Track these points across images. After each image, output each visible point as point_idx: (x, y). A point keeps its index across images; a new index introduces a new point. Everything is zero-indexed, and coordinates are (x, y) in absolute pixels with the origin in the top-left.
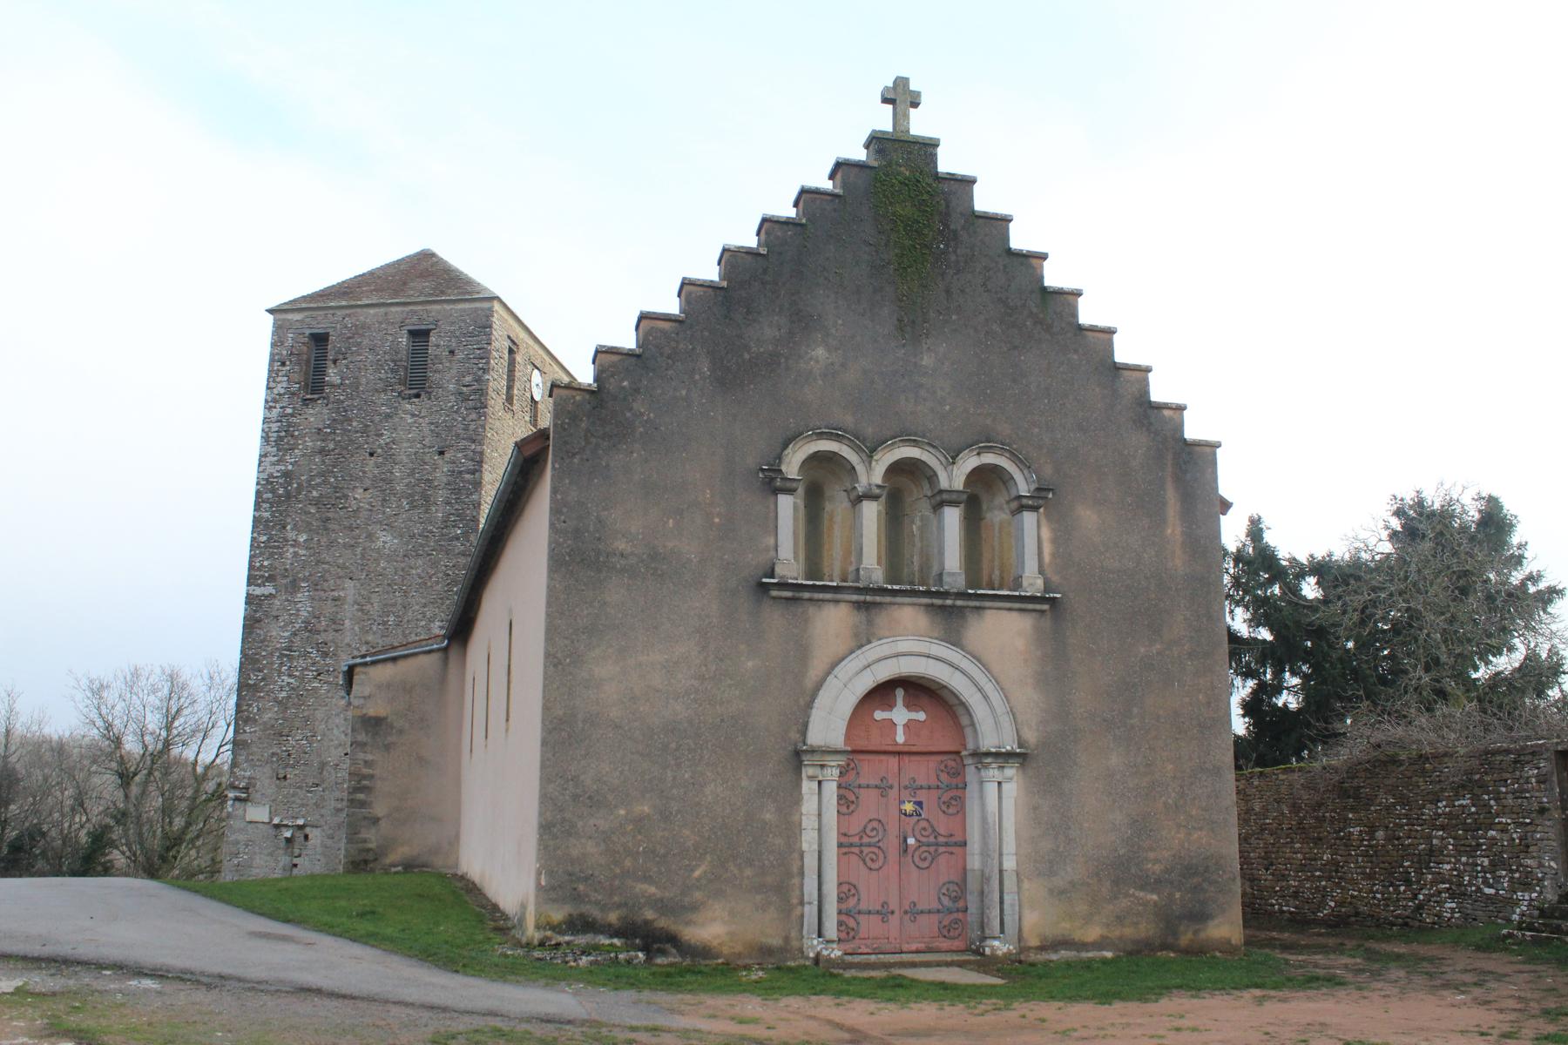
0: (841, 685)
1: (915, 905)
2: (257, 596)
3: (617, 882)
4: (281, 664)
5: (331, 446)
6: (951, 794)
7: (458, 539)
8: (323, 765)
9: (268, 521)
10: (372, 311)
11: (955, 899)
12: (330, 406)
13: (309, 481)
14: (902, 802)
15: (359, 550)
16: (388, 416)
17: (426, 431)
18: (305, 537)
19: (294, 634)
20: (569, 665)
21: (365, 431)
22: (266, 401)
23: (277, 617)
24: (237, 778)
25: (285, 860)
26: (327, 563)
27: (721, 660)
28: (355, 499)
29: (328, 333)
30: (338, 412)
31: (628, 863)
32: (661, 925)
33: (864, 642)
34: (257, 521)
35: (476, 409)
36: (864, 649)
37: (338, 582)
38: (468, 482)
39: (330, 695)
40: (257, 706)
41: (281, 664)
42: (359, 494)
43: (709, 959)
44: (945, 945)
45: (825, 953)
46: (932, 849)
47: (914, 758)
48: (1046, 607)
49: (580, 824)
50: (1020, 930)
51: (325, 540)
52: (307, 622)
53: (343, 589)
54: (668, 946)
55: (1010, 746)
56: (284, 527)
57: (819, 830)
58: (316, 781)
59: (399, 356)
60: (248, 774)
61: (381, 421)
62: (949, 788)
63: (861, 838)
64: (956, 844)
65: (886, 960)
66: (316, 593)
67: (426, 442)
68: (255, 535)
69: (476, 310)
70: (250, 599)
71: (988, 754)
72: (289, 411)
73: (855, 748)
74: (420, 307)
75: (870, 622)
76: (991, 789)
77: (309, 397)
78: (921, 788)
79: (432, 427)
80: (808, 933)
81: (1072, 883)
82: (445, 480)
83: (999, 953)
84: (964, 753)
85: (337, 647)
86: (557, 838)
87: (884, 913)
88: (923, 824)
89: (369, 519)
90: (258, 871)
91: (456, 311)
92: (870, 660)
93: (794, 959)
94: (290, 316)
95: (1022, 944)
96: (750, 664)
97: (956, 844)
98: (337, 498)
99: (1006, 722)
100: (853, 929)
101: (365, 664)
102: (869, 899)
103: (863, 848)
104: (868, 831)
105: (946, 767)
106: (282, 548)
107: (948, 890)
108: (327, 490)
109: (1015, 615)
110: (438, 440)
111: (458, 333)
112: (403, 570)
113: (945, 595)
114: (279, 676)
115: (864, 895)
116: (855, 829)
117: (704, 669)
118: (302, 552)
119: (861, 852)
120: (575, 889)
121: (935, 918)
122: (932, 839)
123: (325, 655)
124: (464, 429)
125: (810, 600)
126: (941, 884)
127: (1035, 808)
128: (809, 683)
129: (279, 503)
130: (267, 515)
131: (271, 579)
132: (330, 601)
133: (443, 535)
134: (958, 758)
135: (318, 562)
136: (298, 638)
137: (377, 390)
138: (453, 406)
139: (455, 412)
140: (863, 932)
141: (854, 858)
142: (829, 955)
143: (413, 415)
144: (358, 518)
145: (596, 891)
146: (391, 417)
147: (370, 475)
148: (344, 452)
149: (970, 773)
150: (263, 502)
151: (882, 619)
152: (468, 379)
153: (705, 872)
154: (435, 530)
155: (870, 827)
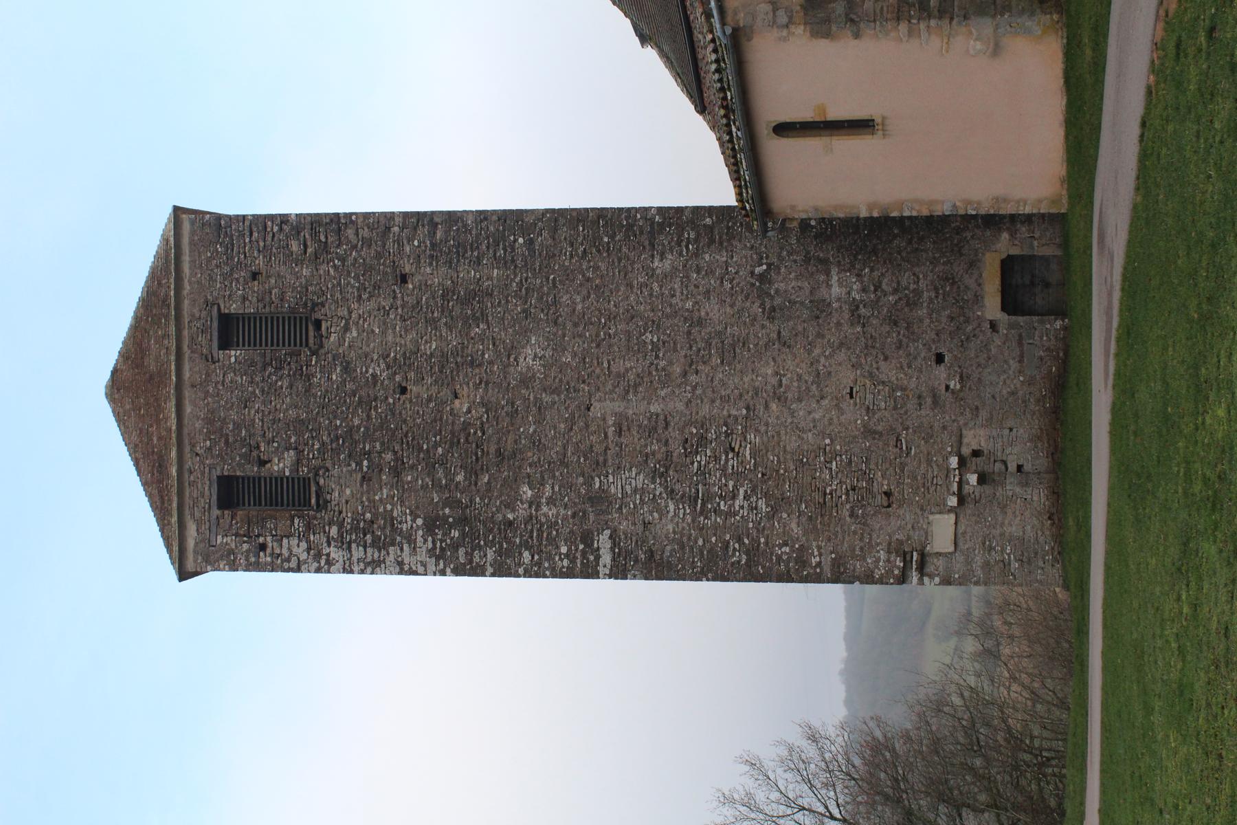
2: (614, 559)
4: (716, 511)
5: (389, 456)
7: (531, 242)
8: (869, 432)
9: (499, 553)
10: (188, 409)
12: (329, 464)
13: (441, 488)
16: (347, 369)
17: (372, 305)
18: (525, 488)
19: (671, 493)
21: (367, 404)
22: (318, 570)
23: (646, 525)
24: (889, 572)
25: (1012, 486)
26: (565, 447)
28: (469, 411)
29: (218, 477)
30: (336, 452)
35: (340, 230)
37: (593, 428)
38: (447, 232)
39: (763, 429)
40: (780, 546)
41: (716, 511)
42: (461, 406)
51: (530, 454)
53: (604, 419)
58: (892, 443)
59: (257, 359)
60: (883, 555)
61: (354, 380)
66: (610, 461)
67: (386, 304)
68: (521, 571)
69: (192, 243)
70: (619, 572)
72: (334, 531)
74: (186, 333)
77: (313, 501)
82: (443, 270)
85: (690, 423)
89: (500, 386)
90: (1028, 528)
91: (193, 274)
94: (191, 543)
98: (467, 440)
106: (542, 525)
110: (384, 285)
111: (227, 269)
112: (576, 325)
114: (736, 514)
123: (703, 440)
124: (370, 246)
131: (587, 539)
132: (622, 440)
133: (526, 265)
136: (677, 487)
138: (335, 266)
139: (343, 260)
143: (347, 329)
146: (348, 363)
147: (434, 389)
148: (399, 434)
150: (471, 562)
152: (295, 246)
154: (518, 279)
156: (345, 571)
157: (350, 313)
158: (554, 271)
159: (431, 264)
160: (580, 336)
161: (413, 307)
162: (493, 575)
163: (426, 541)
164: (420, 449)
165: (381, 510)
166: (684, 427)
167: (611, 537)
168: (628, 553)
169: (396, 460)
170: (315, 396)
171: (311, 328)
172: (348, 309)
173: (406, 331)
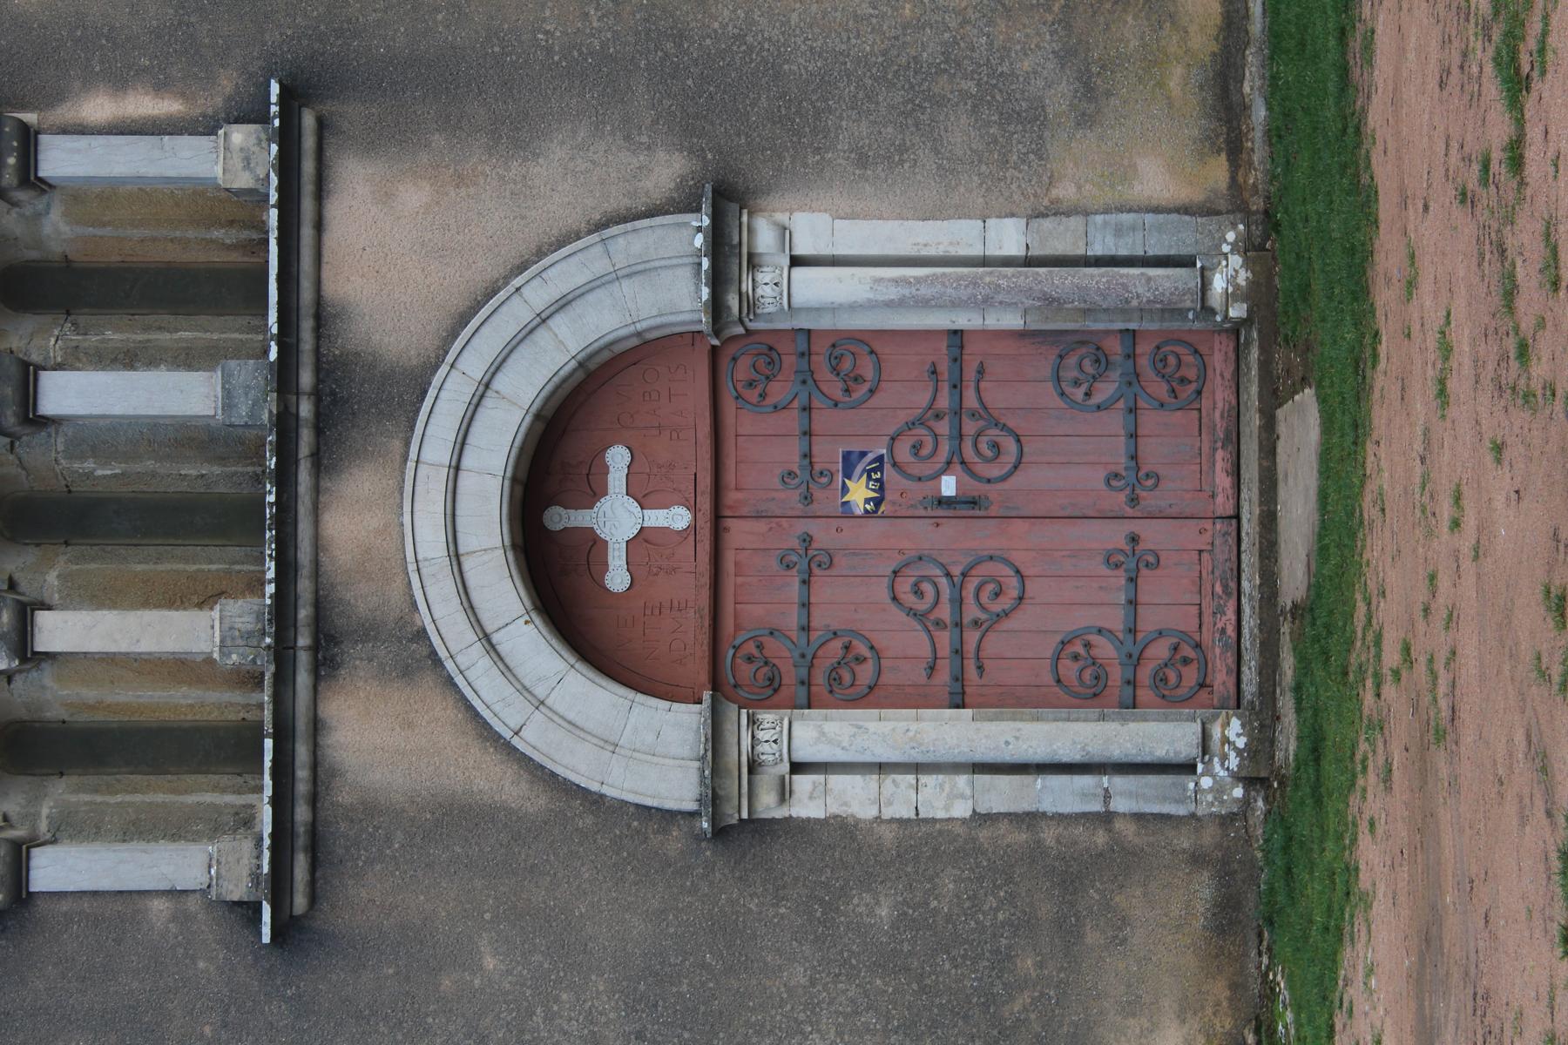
1: (1116, 476)
6: (824, 373)
14: (846, 510)
33: (425, 651)
36: (442, 653)
44: (1219, 396)
45: (1233, 762)
46: (970, 427)
47: (730, 477)
48: (308, 120)
50: (1185, 210)
55: (691, 233)
57: (917, 768)
62: (808, 377)
63: (939, 624)
64: (957, 360)
71: (717, 306)
75: (369, 632)
76: (812, 286)
78: (808, 455)
80: (1177, 801)
81: (1065, 56)
83: (1243, 278)
88: (903, 452)
92: (471, 636)
95: (1222, 205)
96: (490, 963)
97: (957, 360)
99: (633, 243)
100: (1176, 648)
103: (966, 620)
104: (922, 606)
105: (751, 384)
107: (1077, 383)
109: (336, 210)
113: (285, 423)
116: (916, 642)
119: (976, 623)
121: (1150, 420)
122: (943, 427)
125: (314, 800)
126: (1059, 402)
127: (862, 161)
128: (536, 802)
134: (732, 349)
141: (994, 644)
142: (1239, 752)
155: (910, 599)
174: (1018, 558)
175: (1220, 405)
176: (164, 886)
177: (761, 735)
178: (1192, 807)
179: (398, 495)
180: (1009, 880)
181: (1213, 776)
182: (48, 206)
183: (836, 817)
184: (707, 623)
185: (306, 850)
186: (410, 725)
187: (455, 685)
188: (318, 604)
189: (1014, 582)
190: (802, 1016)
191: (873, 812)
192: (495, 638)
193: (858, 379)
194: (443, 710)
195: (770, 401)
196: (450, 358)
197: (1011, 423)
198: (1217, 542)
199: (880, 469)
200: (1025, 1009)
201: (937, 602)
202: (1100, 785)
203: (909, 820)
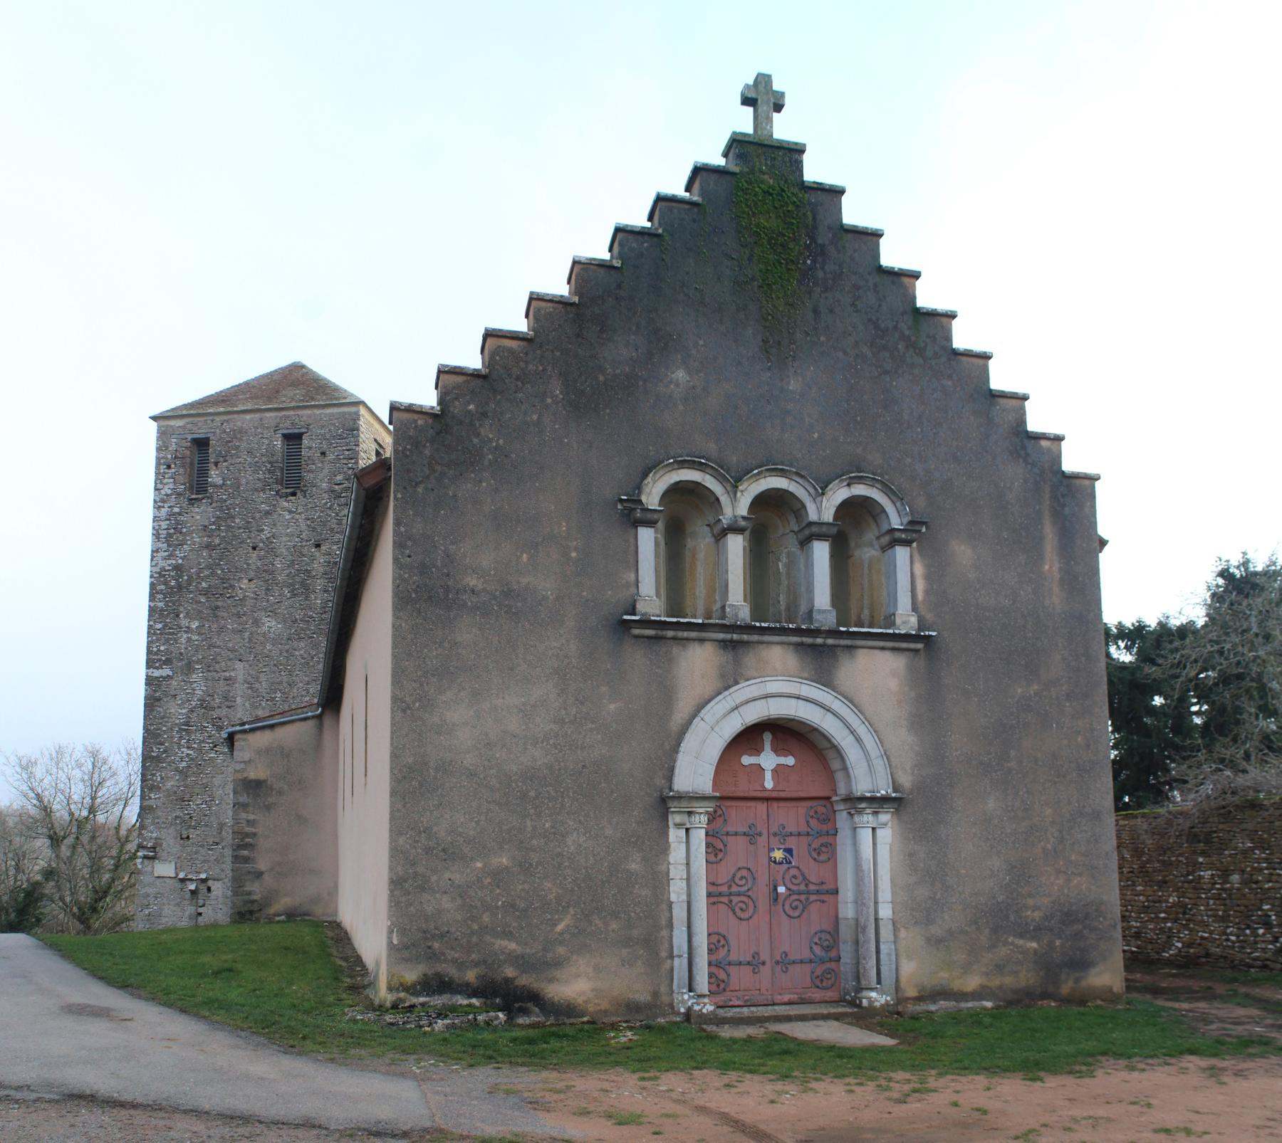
0: (708, 728)
1: (786, 955)
2: (156, 678)
3: (474, 939)
5: (217, 541)
6: (821, 841)
9: (162, 610)
11: (827, 949)
13: (198, 574)
15: (247, 635)
16: (268, 513)
17: (303, 527)
18: (197, 624)
20: (418, 709)
21: (247, 527)
27: (582, 703)
28: (241, 589)
31: (486, 918)
32: (523, 983)
33: (730, 684)
34: (152, 610)
36: (731, 690)
37: (229, 663)
42: (244, 584)
43: (575, 1017)
45: (697, 1008)
46: (803, 897)
47: (782, 804)
49: (434, 878)
52: (202, 700)
54: (530, 1005)
56: (178, 616)
57: (688, 879)
61: (261, 518)
62: (819, 834)
63: (730, 887)
64: (827, 892)
65: (759, 1014)
67: (304, 536)
68: (151, 623)
70: (150, 681)
73: (725, 794)
75: (737, 663)
78: (791, 834)
79: (308, 522)
82: (322, 570)
84: (834, 799)
86: (409, 894)
87: (755, 964)
88: (793, 872)
93: (664, 1016)
96: (612, 707)
97: (827, 892)
98: (224, 588)
100: (723, 981)
101: (244, 732)
102: (739, 949)
103: (732, 897)
104: (737, 880)
105: (816, 812)
106: (176, 634)
107: (820, 939)
108: (214, 581)
110: (315, 534)
112: (287, 651)
115: (733, 942)
116: (724, 877)
117: (564, 712)
118: (195, 637)
119: (731, 901)
120: (429, 947)
121: (807, 968)
122: (802, 887)
125: (674, 638)
126: (812, 933)
128: (674, 725)
129: (172, 594)
130: (161, 605)
131: (168, 662)
132: (222, 681)
133: (322, 620)
134: (829, 806)
135: (211, 646)
137: (256, 490)
139: (330, 508)
140: (734, 983)
141: (723, 908)
142: (701, 1010)
143: (290, 512)
144: (245, 606)
145: (452, 949)
146: (271, 514)
147: (253, 567)
148: (229, 547)
149: (842, 819)
150: (157, 593)
151: (749, 659)
152: (339, 478)
153: (568, 926)
154: (314, 615)
155: (739, 875)
156: (155, 517)
157: (300, 514)
158: (318, 637)
159: (325, 562)
160: (281, 654)
161: (301, 552)
162: (150, 606)
163: (169, 565)
164: (220, 560)
165: (188, 538)
166: (228, 718)
167: (168, 676)
168: (159, 686)
169: (215, 546)
170: (252, 495)
171: (291, 490)
172: (302, 513)
173: (287, 549)
174: (755, 917)
175: (813, 995)
176: (640, 579)
177: (702, 816)
178: (676, 991)
179: (788, 675)
180: (646, 918)
181: (688, 1000)
182: (876, 550)
183: (670, 846)
184: (731, 795)
185: (656, 634)
186: (703, 677)
187: (718, 695)
188: (747, 643)
189: (747, 916)
190: (592, 833)
191: (672, 861)
192: (736, 711)
193: (819, 854)
194: (708, 691)
195: (810, 820)
196: (839, 696)
197: (805, 914)
198: (764, 997)
199: (787, 863)
200: (596, 925)
201: (738, 885)
202: (684, 953)
203: (669, 876)
